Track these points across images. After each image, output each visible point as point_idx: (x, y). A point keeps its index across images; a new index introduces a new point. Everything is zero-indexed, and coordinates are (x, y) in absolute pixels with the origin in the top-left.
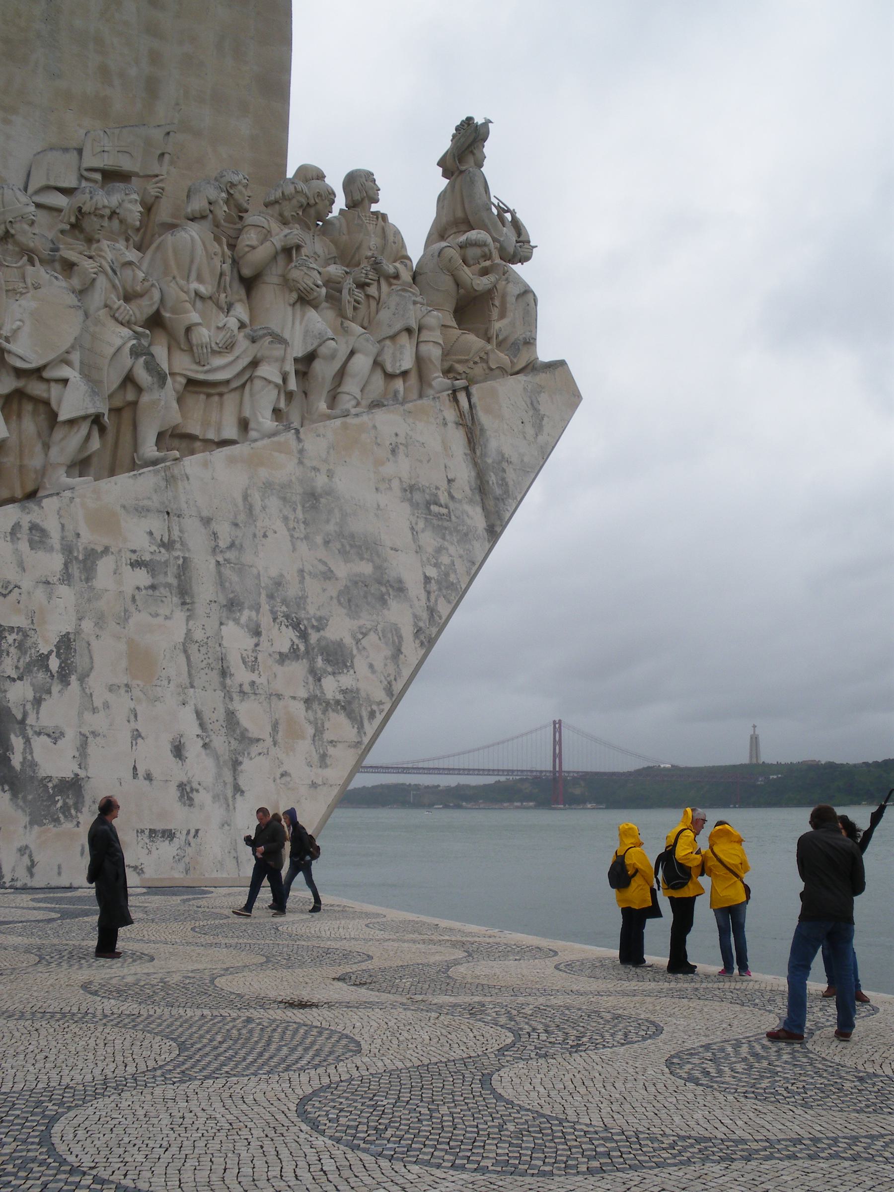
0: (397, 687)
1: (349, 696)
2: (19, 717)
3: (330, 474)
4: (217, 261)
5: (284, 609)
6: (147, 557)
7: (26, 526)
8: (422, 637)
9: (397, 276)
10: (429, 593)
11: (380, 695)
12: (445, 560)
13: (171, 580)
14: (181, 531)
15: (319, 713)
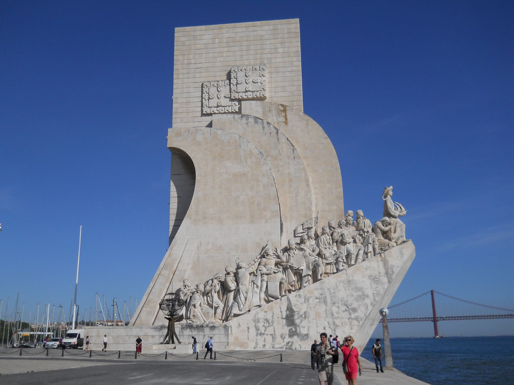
0: (367, 314)
1: (357, 317)
2: (298, 325)
3: (353, 277)
4: (328, 241)
5: (344, 303)
6: (318, 297)
7: (298, 295)
8: (372, 305)
9: (368, 232)
10: (374, 296)
11: (363, 316)
12: (378, 289)
13: (323, 300)
14: (324, 291)
15: (351, 321)
